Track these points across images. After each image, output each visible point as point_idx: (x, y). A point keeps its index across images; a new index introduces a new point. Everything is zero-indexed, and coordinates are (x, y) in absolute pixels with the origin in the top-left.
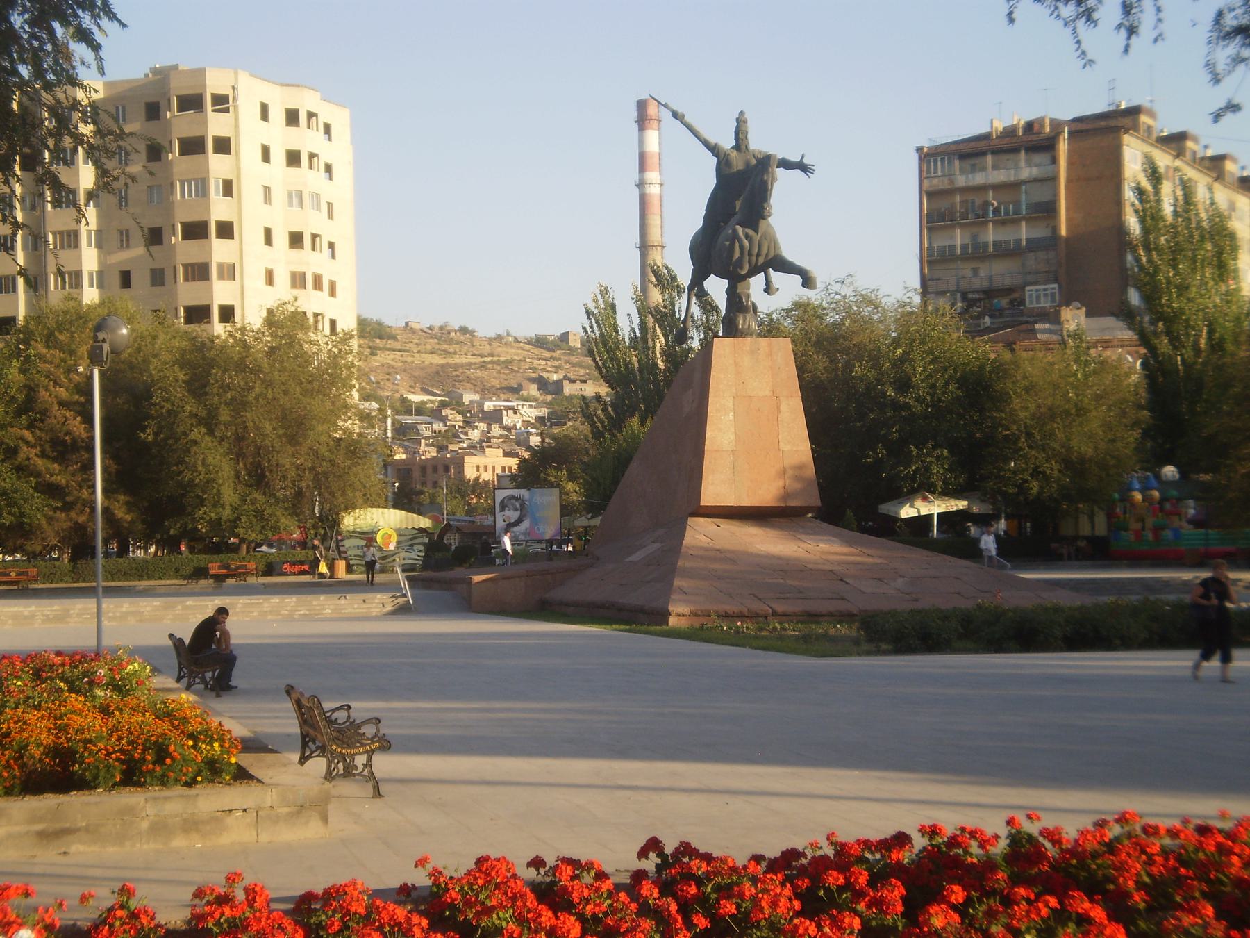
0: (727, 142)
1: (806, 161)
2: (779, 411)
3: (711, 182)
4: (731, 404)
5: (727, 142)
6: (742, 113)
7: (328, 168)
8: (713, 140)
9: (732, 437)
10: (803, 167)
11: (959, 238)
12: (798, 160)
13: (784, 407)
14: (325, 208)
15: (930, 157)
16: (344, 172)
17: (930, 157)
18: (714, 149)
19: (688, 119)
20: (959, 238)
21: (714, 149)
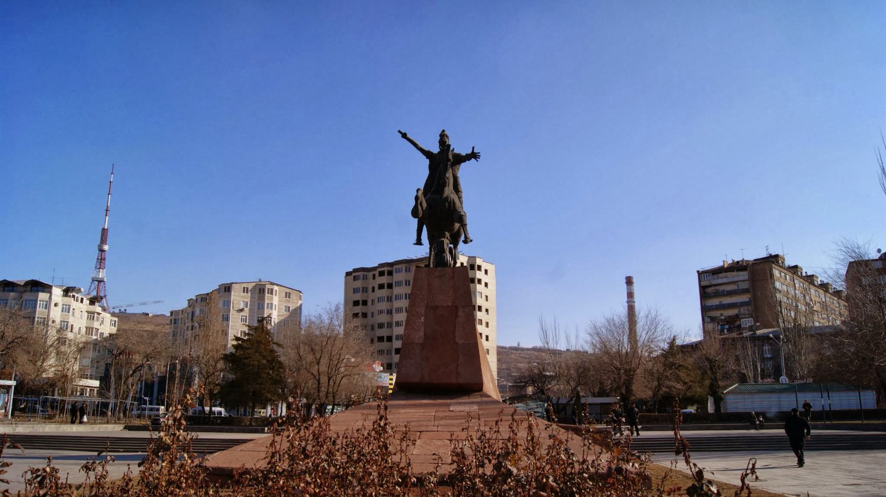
0: (435, 149)
1: (475, 151)
2: (457, 316)
3: (426, 173)
4: (423, 311)
5: (435, 149)
6: (444, 131)
7: (486, 285)
8: (426, 149)
9: (422, 334)
10: (474, 155)
11: (715, 302)
12: (470, 152)
13: (461, 313)
14: (484, 297)
15: (700, 274)
16: (492, 286)
17: (700, 274)
18: (427, 154)
19: (408, 136)
20: (715, 302)
21: (427, 154)
